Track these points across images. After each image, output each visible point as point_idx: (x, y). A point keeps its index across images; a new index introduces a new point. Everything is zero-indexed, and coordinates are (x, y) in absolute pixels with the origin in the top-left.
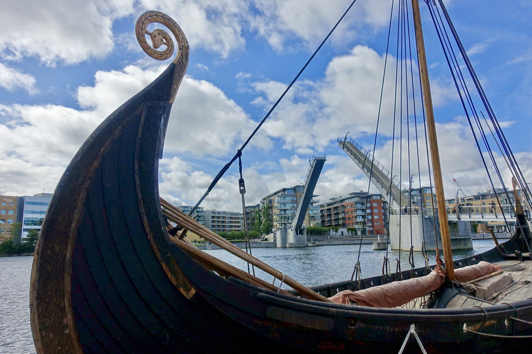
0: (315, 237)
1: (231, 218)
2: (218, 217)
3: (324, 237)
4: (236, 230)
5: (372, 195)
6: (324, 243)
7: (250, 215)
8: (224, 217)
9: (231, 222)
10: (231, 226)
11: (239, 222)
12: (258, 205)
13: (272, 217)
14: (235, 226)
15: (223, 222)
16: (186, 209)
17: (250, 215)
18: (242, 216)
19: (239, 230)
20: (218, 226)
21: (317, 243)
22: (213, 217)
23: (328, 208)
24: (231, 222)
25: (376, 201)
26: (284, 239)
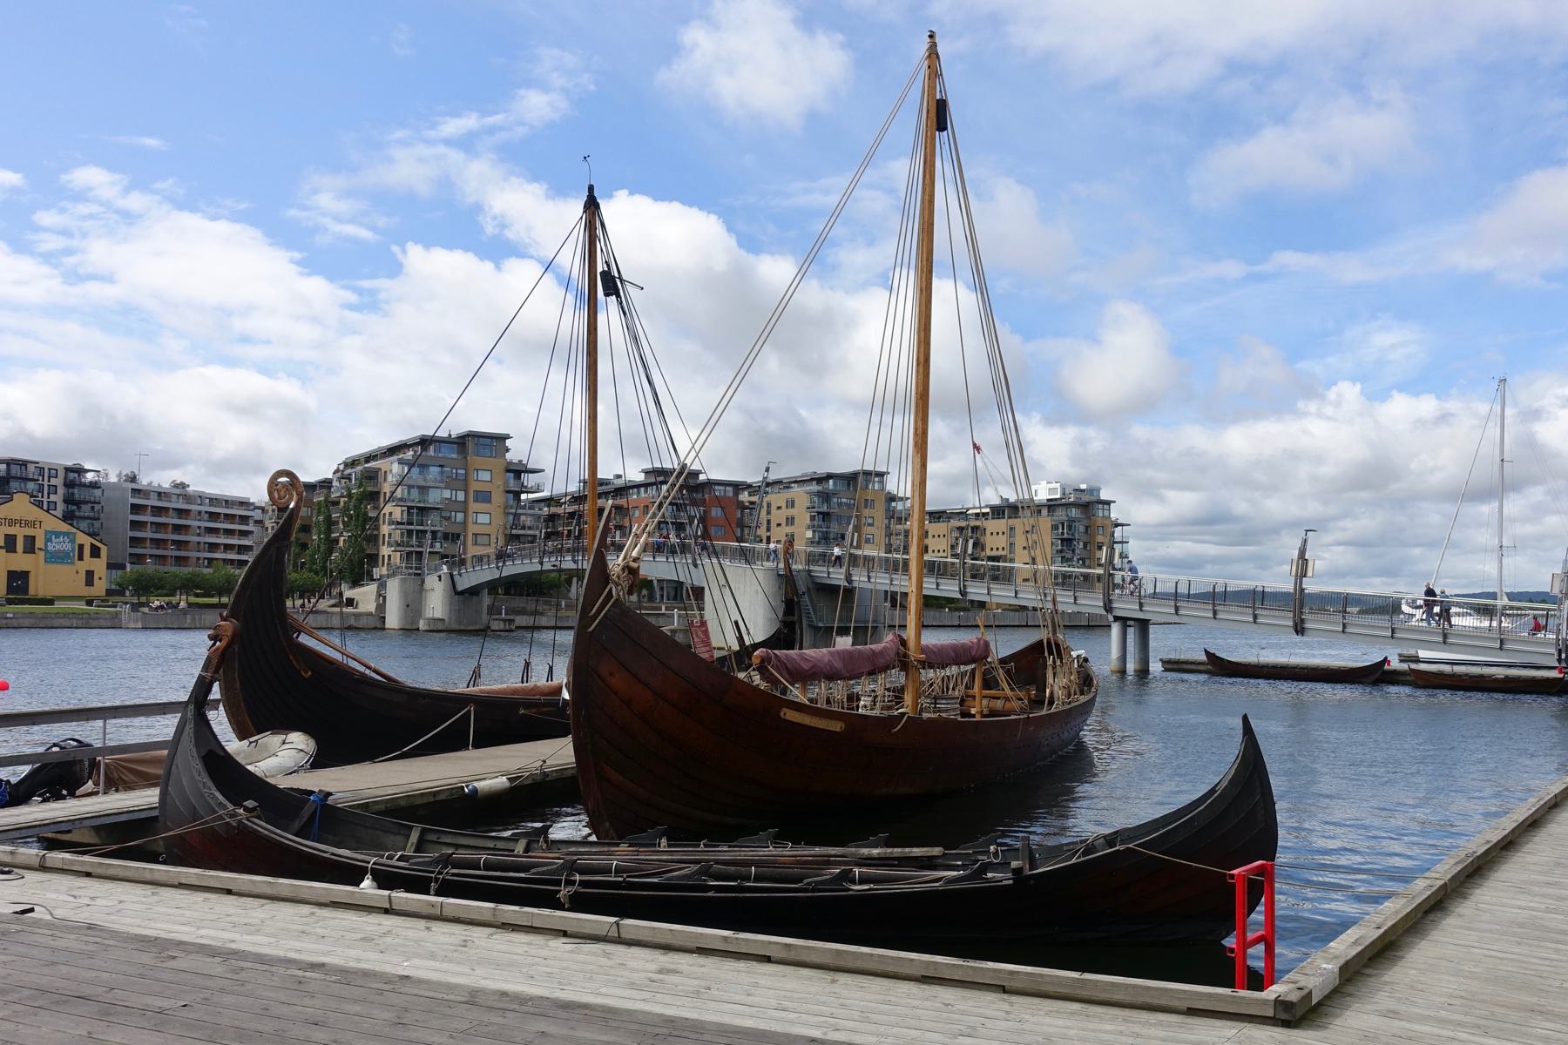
0: (519, 602)
3: (546, 603)
4: (232, 561)
5: (710, 484)
6: (544, 621)
12: (326, 484)
13: (377, 528)
16: (15, 470)
18: (257, 515)
21: (520, 620)
23: (570, 509)
25: (719, 501)
26: (413, 606)
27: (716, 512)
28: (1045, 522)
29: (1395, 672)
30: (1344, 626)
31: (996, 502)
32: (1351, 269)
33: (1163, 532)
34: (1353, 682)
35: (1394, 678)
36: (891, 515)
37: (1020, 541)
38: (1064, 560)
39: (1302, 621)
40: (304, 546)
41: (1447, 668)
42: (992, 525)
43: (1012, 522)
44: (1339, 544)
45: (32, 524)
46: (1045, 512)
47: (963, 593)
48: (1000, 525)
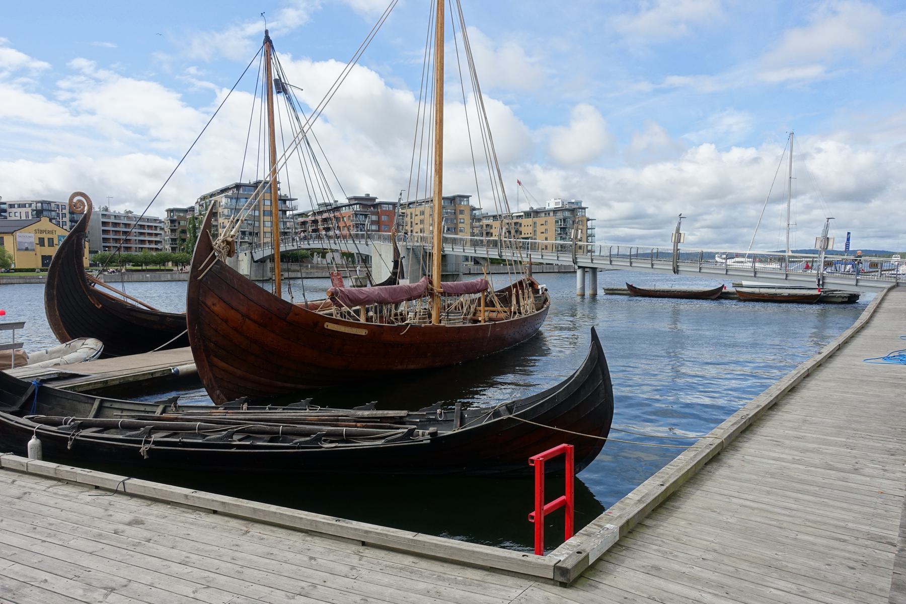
1: (142, 227)
2: (115, 225)
4: (152, 249)
7: (177, 224)
8: (127, 225)
9: (141, 234)
10: (143, 242)
11: (156, 235)
12: (192, 209)
14: (150, 242)
15: (125, 233)
17: (177, 224)
18: (162, 225)
19: (157, 249)
20: (116, 240)
22: (104, 224)
24: (141, 234)
27: (384, 218)
28: (552, 219)
29: (728, 293)
30: (700, 268)
31: (527, 209)
32: (708, 85)
33: (611, 224)
34: (703, 299)
35: (726, 296)
36: (474, 218)
37: (540, 229)
38: (562, 239)
39: (678, 266)
40: (184, 240)
41: (757, 290)
42: (525, 221)
43: (535, 219)
44: (703, 227)
45: (51, 232)
46: (552, 214)
47: (500, 256)
48: (529, 221)
